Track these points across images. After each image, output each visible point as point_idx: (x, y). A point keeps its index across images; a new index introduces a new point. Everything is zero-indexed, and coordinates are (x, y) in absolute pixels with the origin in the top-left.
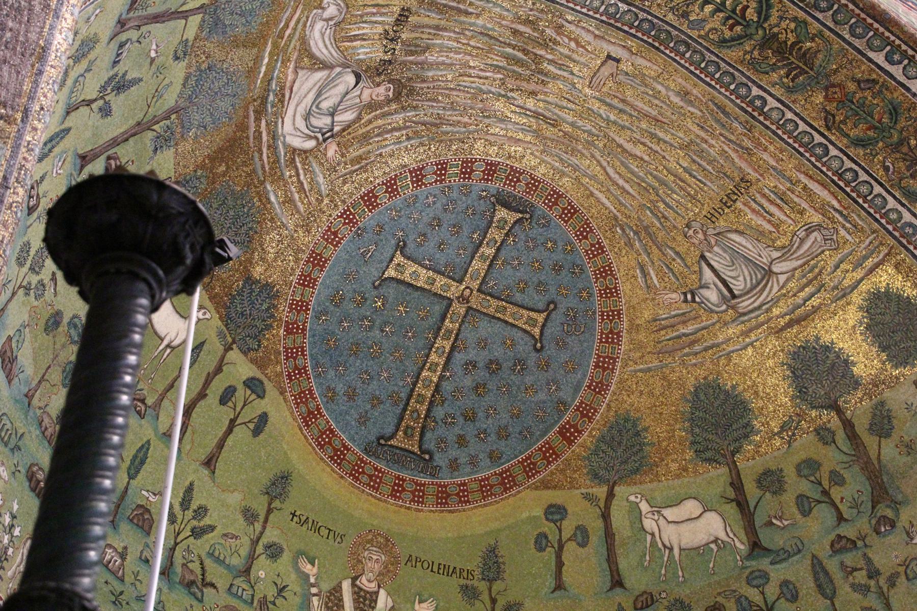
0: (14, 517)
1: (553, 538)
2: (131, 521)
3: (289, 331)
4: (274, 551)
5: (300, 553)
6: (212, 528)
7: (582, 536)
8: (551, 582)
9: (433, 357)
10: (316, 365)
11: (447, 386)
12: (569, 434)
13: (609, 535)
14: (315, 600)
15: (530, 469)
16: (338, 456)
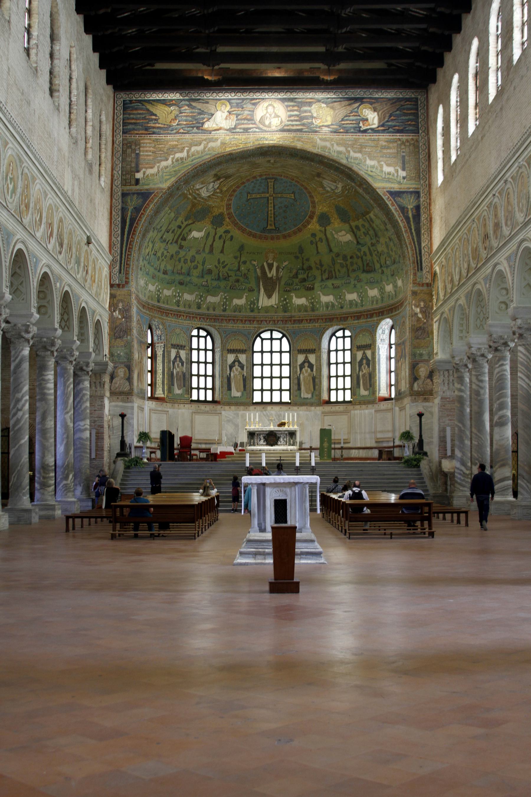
0: (179, 293)
1: (314, 241)
2: (207, 274)
3: (229, 218)
4: (245, 263)
5: (251, 260)
6: (227, 264)
7: (321, 240)
8: (316, 252)
9: (270, 209)
10: (240, 221)
11: (277, 213)
12: (311, 217)
13: (327, 240)
14: (258, 270)
15: (305, 226)
16: (254, 236)
